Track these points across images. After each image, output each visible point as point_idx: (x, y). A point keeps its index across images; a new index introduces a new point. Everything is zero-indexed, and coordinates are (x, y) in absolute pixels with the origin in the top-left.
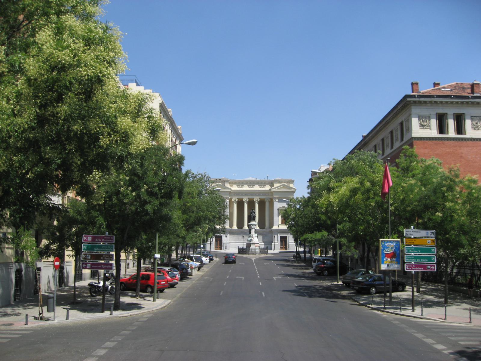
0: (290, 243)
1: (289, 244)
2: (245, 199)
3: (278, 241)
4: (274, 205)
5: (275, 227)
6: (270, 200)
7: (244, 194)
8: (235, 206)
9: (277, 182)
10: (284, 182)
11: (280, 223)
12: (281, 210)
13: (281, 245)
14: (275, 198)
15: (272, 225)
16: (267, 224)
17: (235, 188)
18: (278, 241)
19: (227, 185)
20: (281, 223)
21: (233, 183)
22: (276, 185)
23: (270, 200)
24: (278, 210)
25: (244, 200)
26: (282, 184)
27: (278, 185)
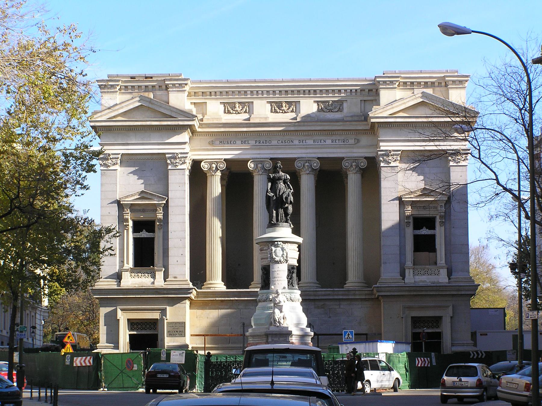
6: (364, 164)
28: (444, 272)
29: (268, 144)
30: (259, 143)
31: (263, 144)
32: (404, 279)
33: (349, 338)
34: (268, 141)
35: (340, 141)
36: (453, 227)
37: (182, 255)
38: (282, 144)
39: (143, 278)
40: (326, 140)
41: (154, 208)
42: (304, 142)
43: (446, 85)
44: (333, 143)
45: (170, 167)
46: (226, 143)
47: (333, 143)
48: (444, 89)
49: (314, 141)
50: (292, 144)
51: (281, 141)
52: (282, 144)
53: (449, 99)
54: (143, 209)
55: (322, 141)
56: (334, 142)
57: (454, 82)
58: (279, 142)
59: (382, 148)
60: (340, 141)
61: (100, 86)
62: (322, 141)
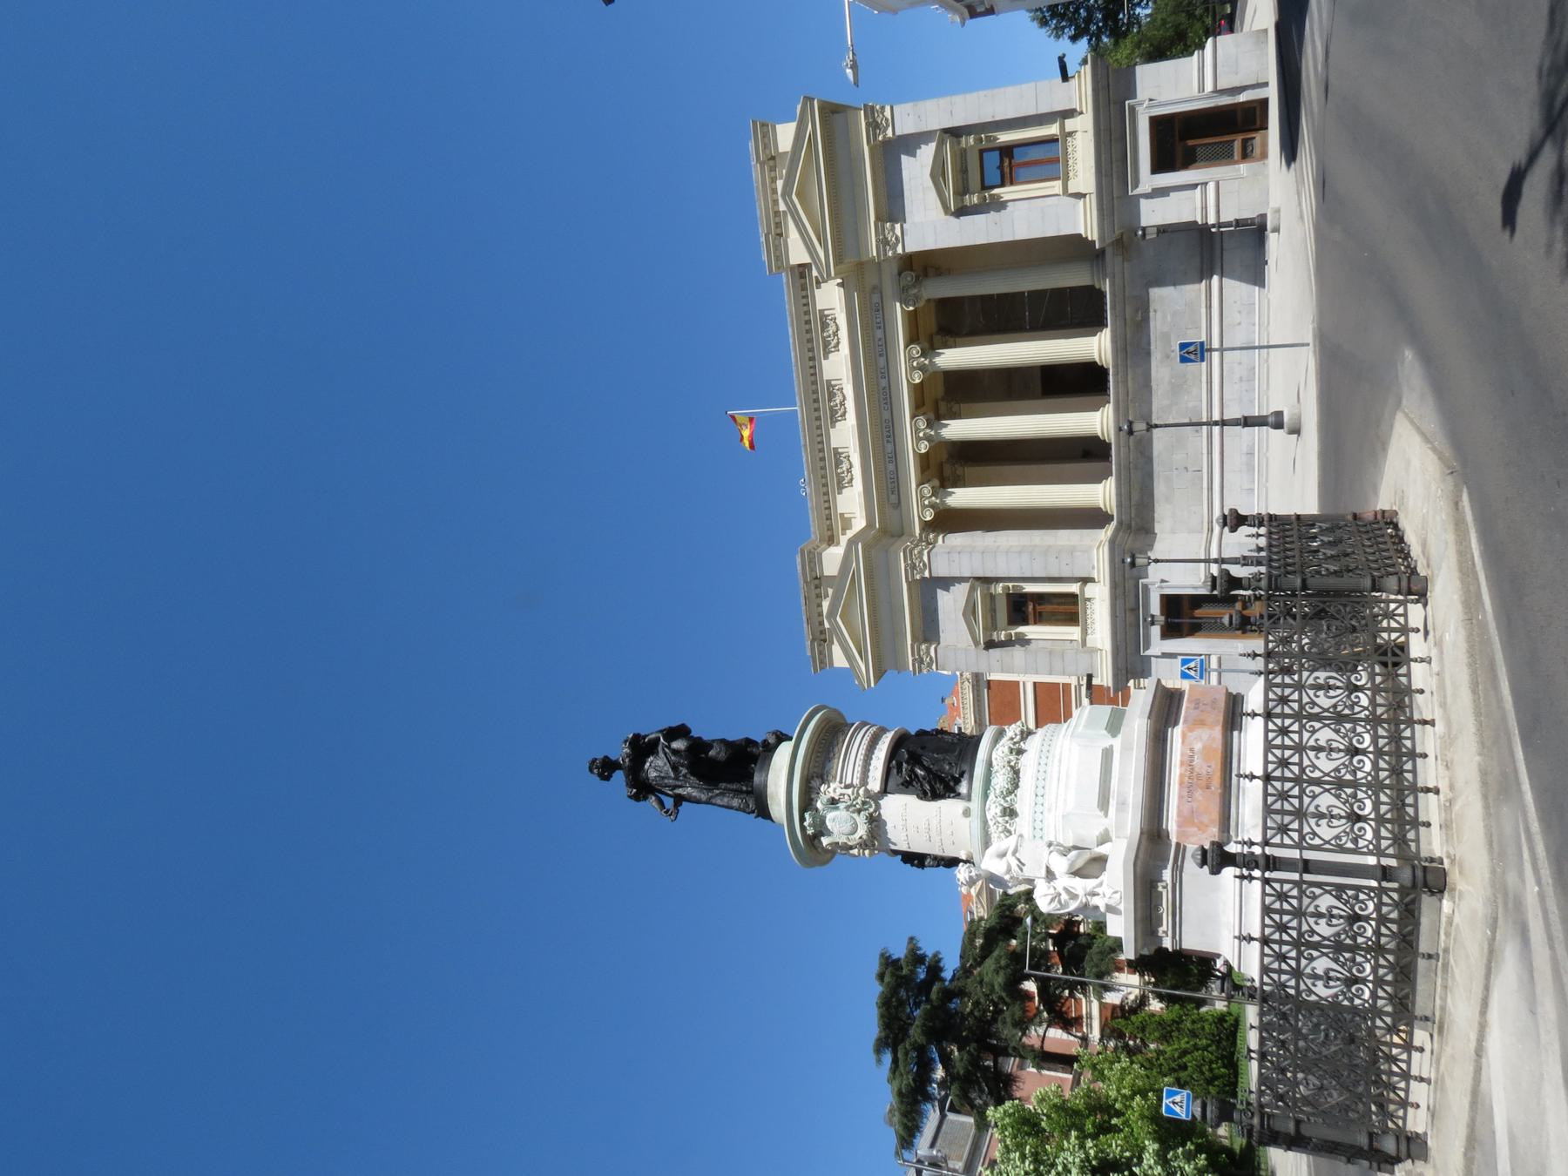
0: (1209, 87)
1: (1219, 92)
2: (919, 439)
3: (1194, 186)
4: (929, 244)
5: (1083, 221)
7: (889, 447)
8: (963, 497)
9: (777, 247)
10: (774, 191)
11: (1056, 186)
12: (962, 190)
13: (1222, 156)
14: (884, 242)
15: (1071, 248)
16: (1074, 277)
17: (852, 503)
18: (1194, 186)
19: (832, 559)
20: (1058, 178)
21: (829, 518)
22: (798, 254)
23: (909, 277)
24: (961, 211)
25: (924, 448)
26: (782, 207)
27: (793, 236)
28: (1070, 124)
29: (890, 423)
30: (890, 437)
31: (891, 432)
32: (1084, 196)
33: (1181, 1102)
36: (993, 117)
37: (1057, 558)
39: (1094, 616)
41: (991, 599)
42: (883, 371)
43: (773, 158)
45: (927, 574)
48: (778, 159)
53: (788, 152)
54: (991, 611)
55: (880, 343)
57: (766, 146)
59: (875, 254)
61: (821, 669)
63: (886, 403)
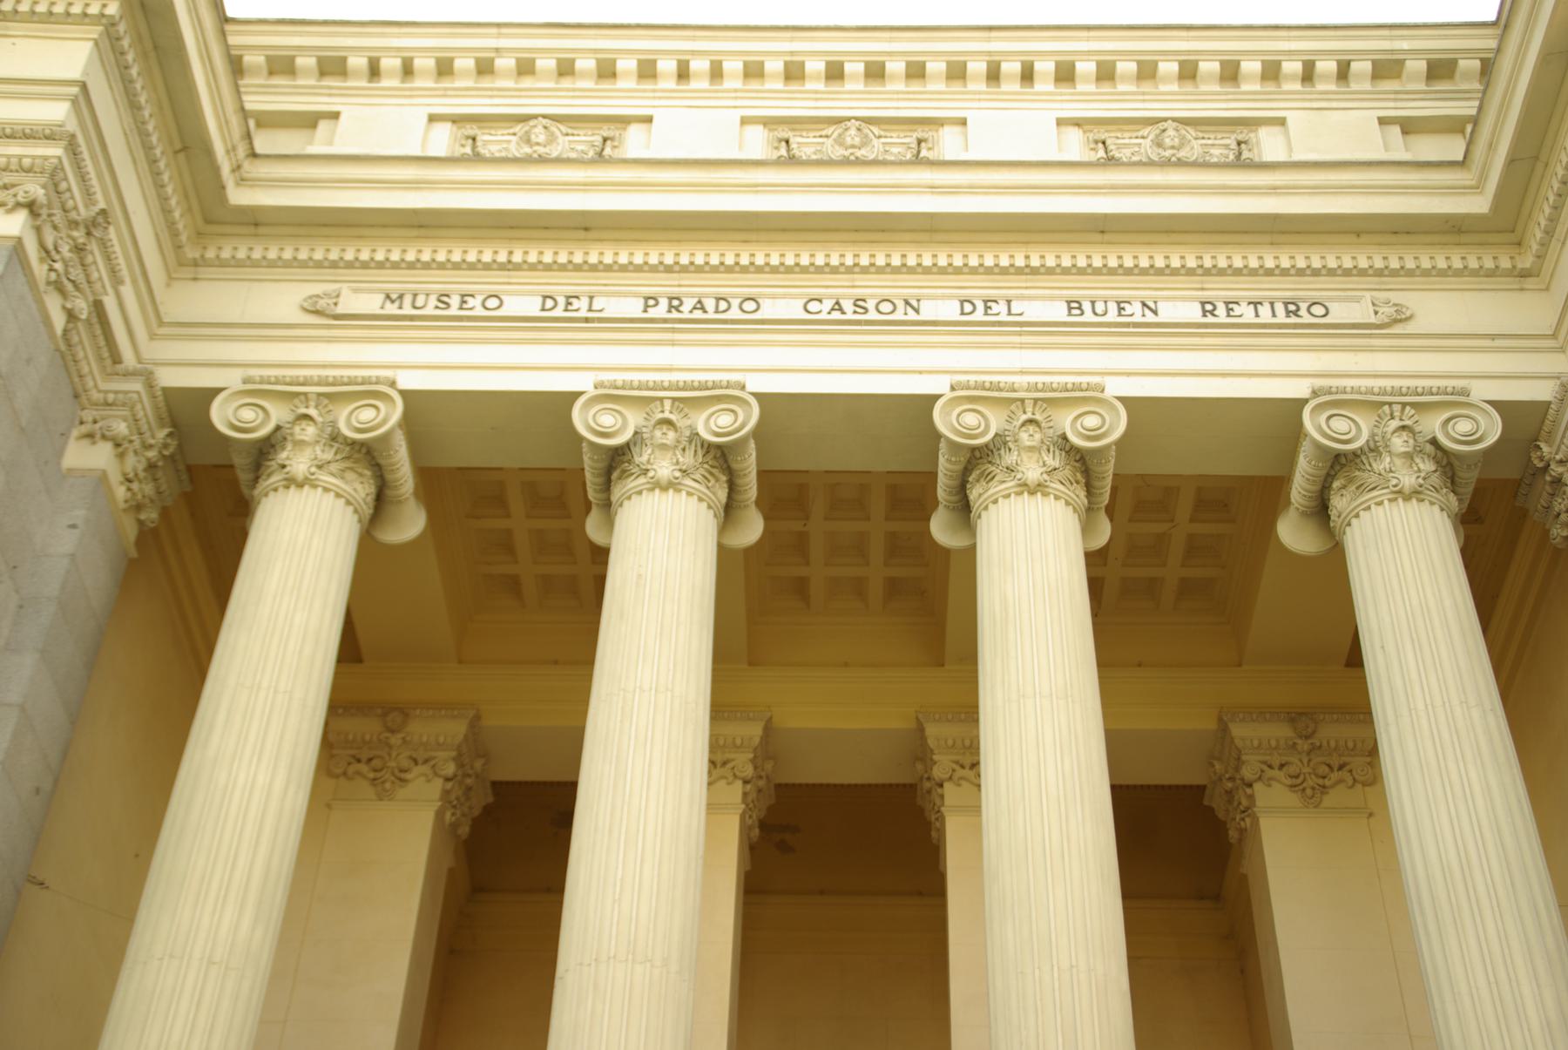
29: (734, 313)
31: (698, 314)
34: (735, 303)
35: (1265, 311)
38: (836, 315)
40: (1159, 304)
44: (1210, 319)
46: (433, 301)
47: (1210, 319)
49: (1073, 305)
50: (912, 316)
51: (828, 304)
52: (836, 315)
56: (1221, 310)
58: (813, 306)
60: (1265, 311)
62: (1136, 308)
63: (838, 307)
